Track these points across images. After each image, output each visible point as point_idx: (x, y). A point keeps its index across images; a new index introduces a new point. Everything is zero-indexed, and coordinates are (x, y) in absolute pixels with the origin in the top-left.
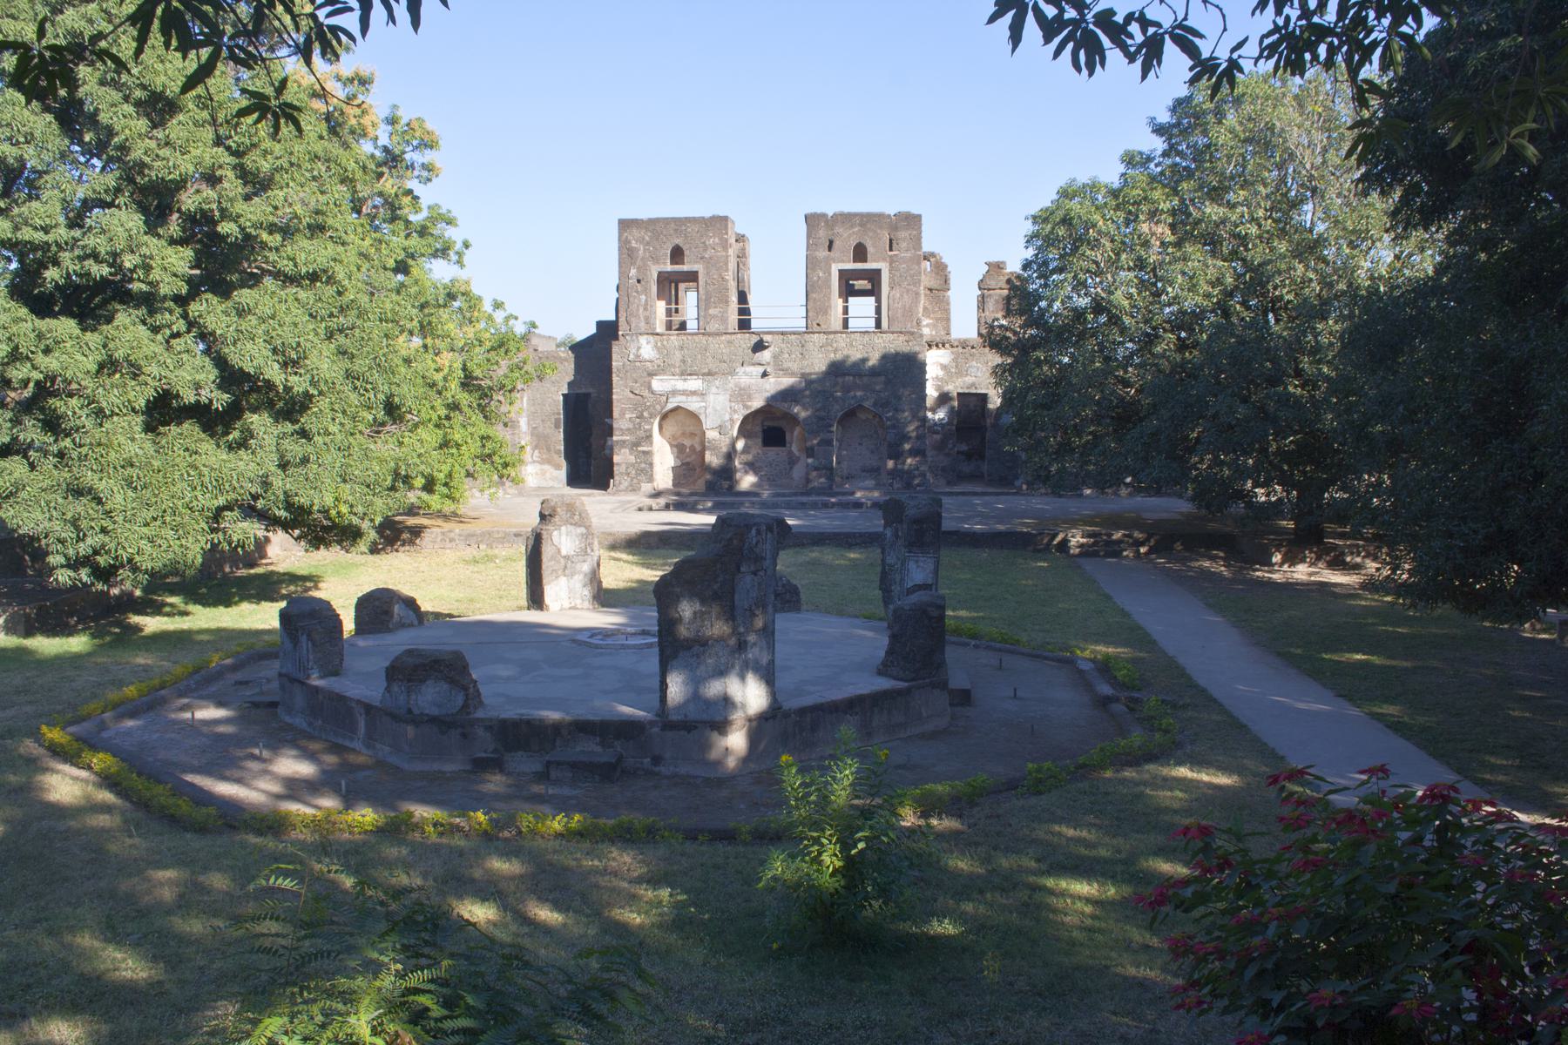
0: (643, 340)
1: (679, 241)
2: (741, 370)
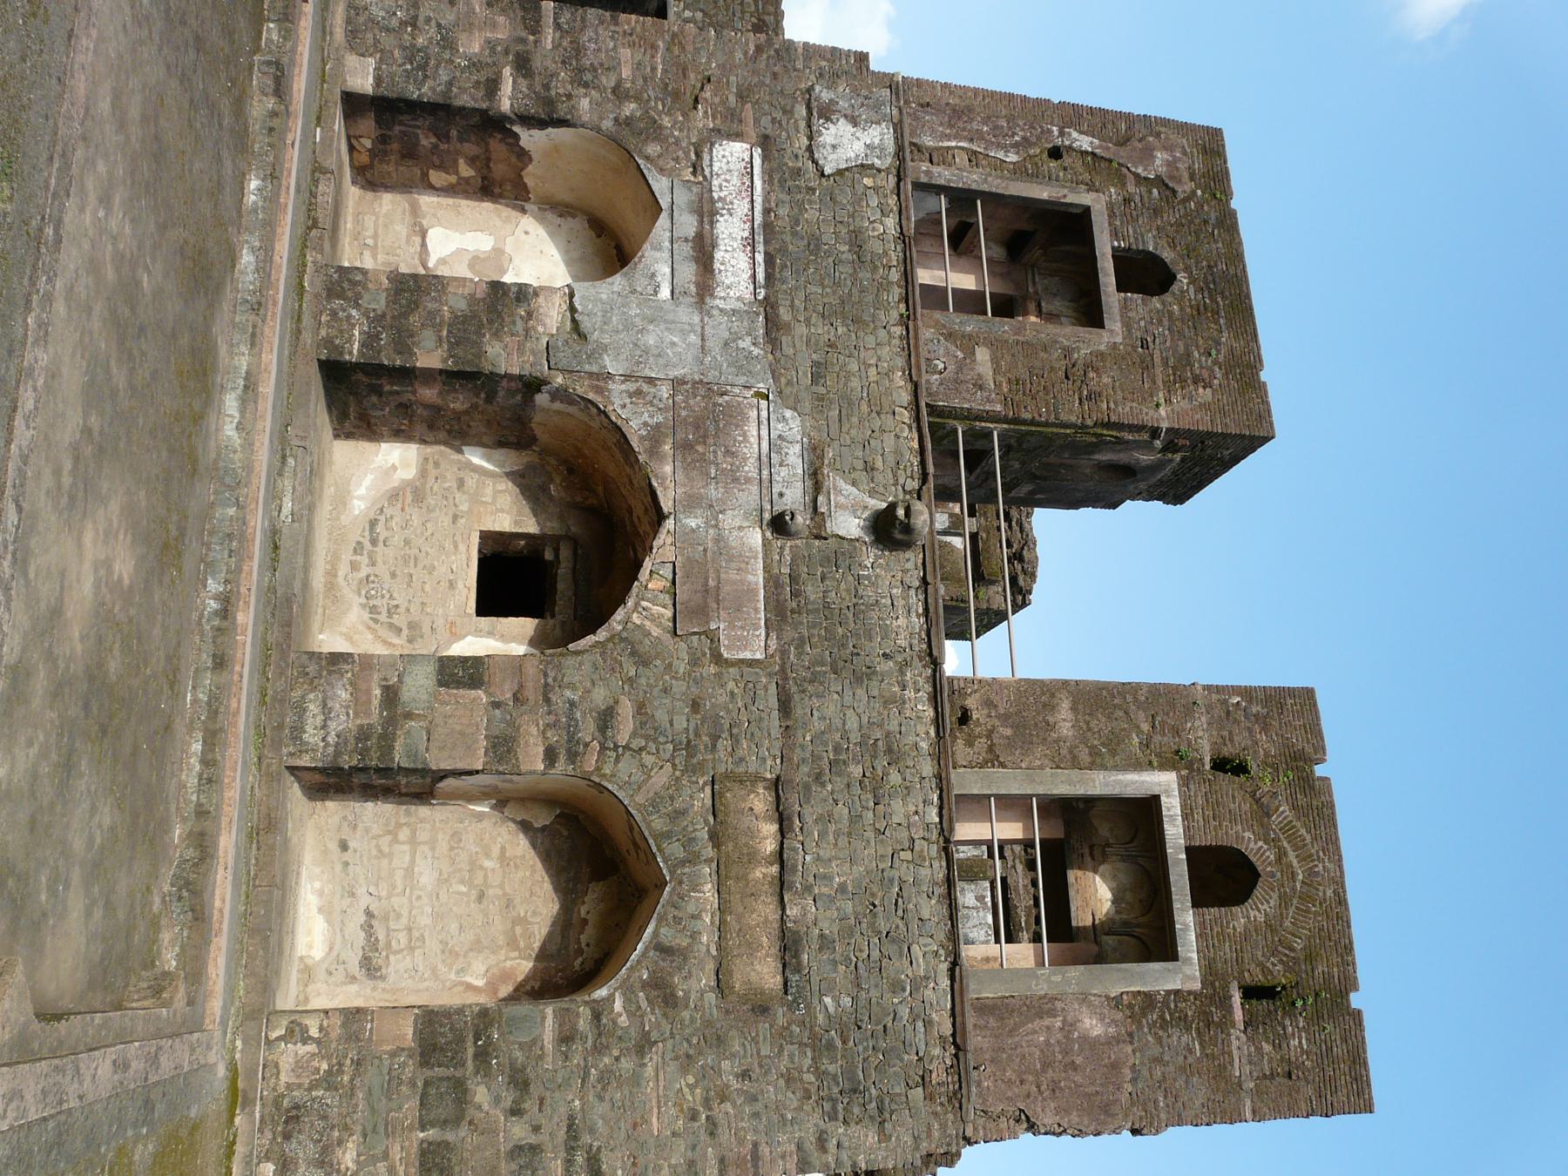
0: (879, 135)
2: (792, 425)
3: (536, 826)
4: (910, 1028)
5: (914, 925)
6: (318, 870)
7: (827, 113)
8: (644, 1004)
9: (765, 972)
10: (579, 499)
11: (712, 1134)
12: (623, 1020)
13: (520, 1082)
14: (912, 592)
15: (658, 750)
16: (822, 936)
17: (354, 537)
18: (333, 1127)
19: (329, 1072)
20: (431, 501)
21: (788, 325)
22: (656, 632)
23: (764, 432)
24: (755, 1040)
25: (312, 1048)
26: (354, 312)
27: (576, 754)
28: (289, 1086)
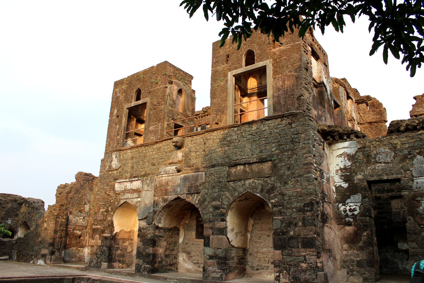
1: (138, 86)
3: (253, 223)
4: (279, 129)
5: (257, 130)
6: (262, 275)
7: (110, 167)
8: (273, 195)
9: (267, 166)
10: (189, 216)
11: (301, 176)
12: (276, 200)
13: (289, 224)
14: (193, 139)
15: (222, 195)
16: (260, 153)
17: (197, 268)
18: (298, 269)
19: (286, 270)
20: (190, 250)
21: (145, 172)
22: (199, 197)
23: (164, 175)
24: (281, 167)
25: (281, 274)
26: (143, 266)
27: (222, 214)
28: (289, 280)
